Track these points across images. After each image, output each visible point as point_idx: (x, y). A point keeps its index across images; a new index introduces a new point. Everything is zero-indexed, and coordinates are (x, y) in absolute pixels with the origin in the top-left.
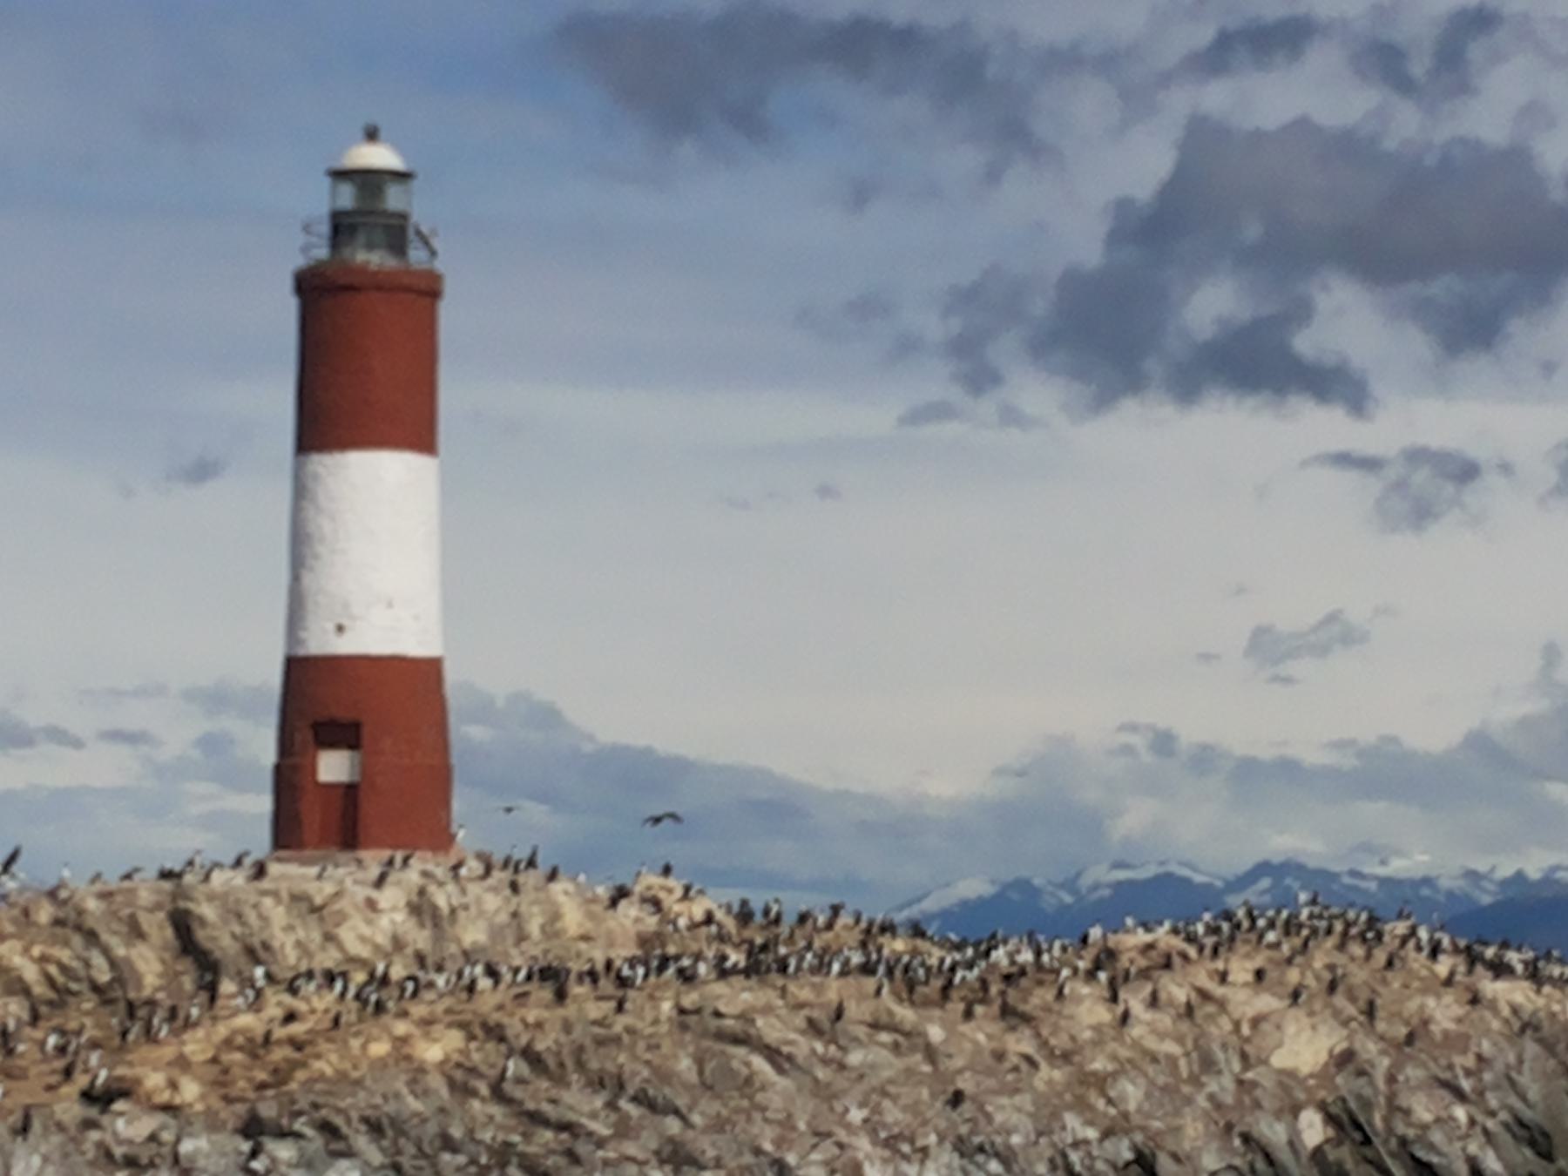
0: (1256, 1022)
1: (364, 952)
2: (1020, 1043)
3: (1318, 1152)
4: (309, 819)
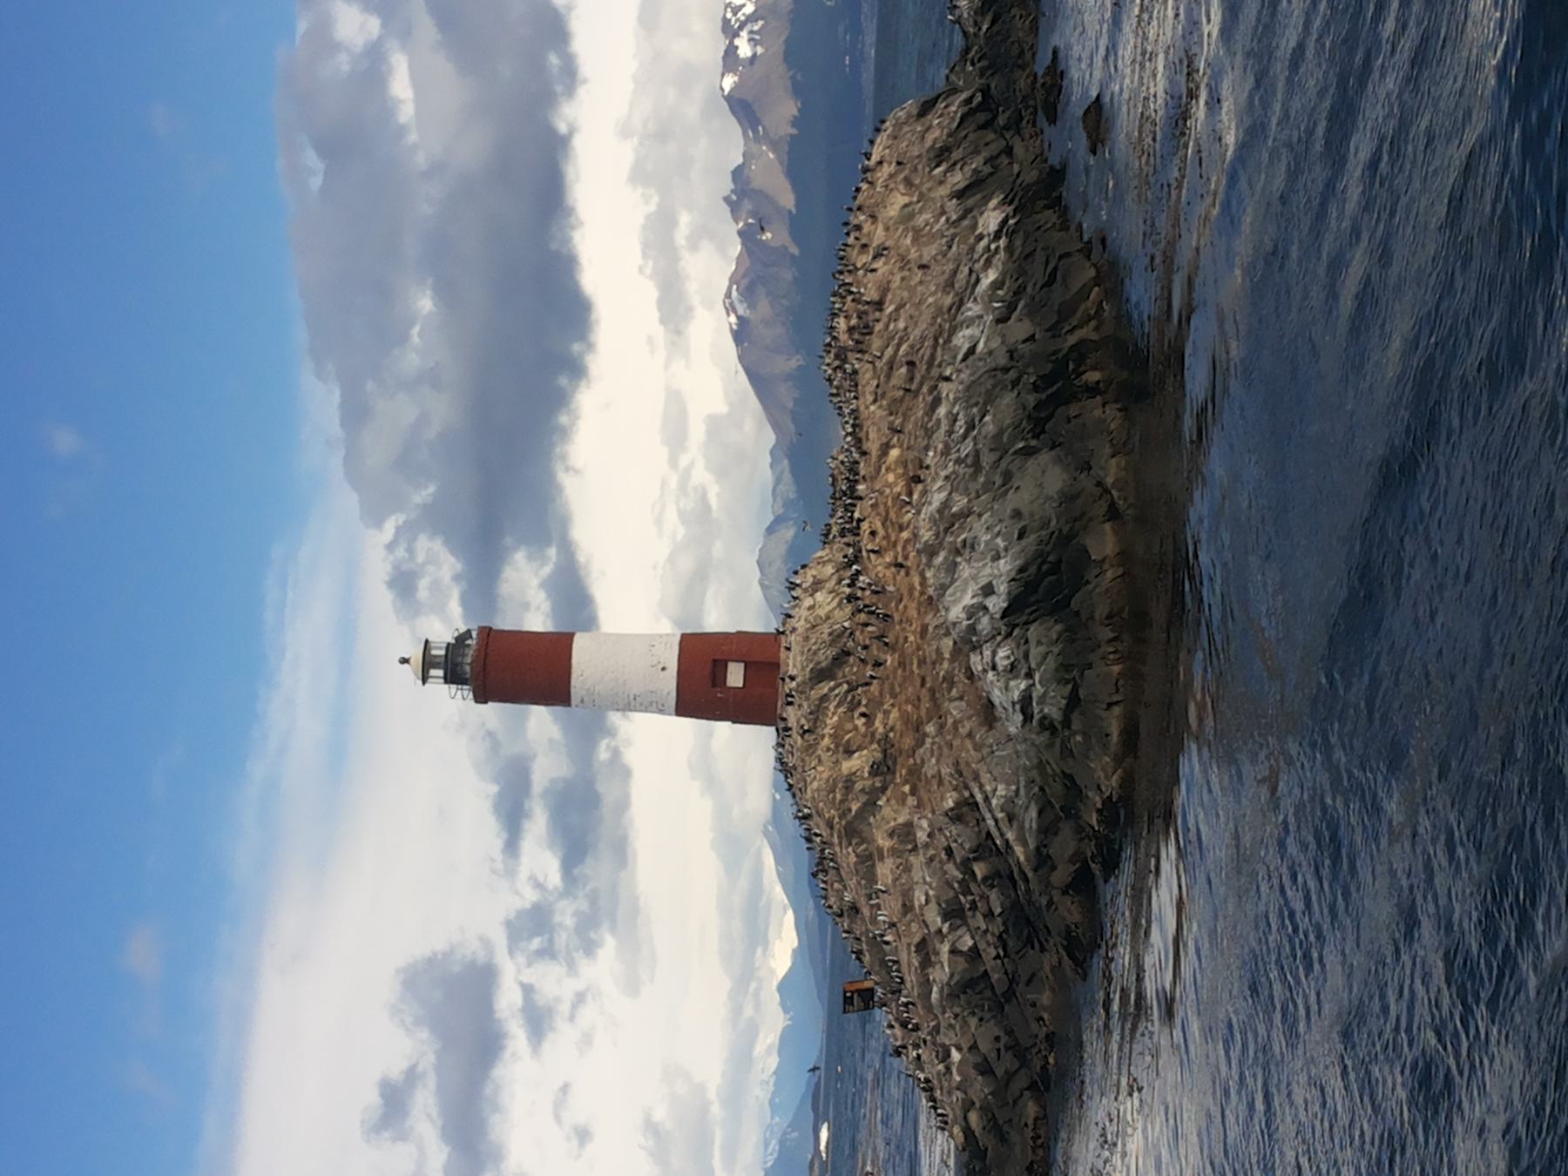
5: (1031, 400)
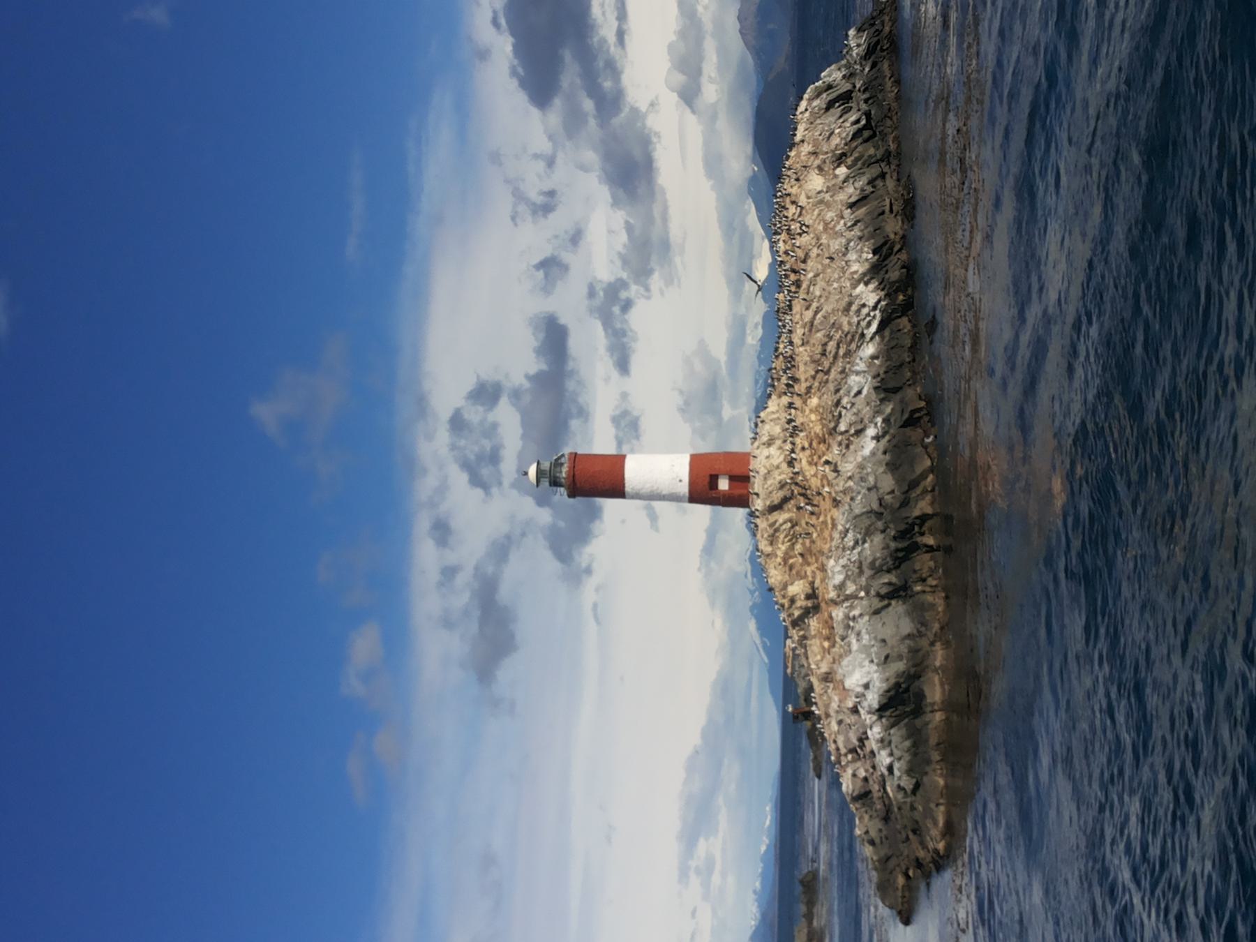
0: (808, 198)
1: (782, 458)
2: (815, 251)
3: (848, 168)
4: (739, 499)
5: (893, 545)
